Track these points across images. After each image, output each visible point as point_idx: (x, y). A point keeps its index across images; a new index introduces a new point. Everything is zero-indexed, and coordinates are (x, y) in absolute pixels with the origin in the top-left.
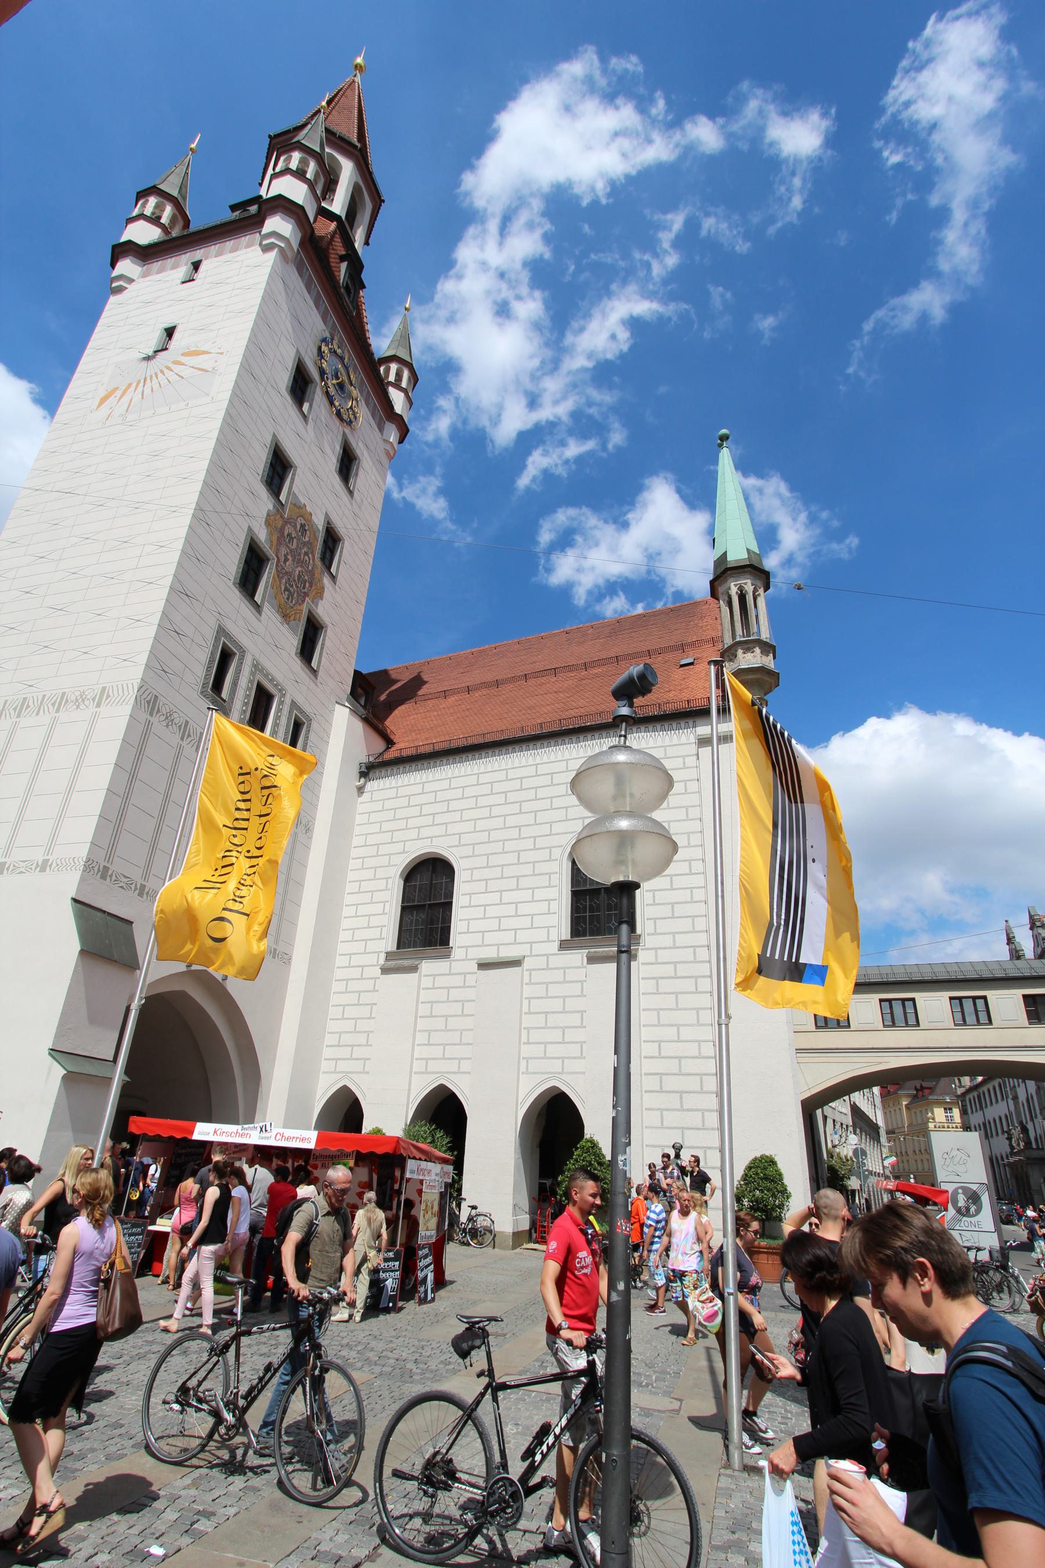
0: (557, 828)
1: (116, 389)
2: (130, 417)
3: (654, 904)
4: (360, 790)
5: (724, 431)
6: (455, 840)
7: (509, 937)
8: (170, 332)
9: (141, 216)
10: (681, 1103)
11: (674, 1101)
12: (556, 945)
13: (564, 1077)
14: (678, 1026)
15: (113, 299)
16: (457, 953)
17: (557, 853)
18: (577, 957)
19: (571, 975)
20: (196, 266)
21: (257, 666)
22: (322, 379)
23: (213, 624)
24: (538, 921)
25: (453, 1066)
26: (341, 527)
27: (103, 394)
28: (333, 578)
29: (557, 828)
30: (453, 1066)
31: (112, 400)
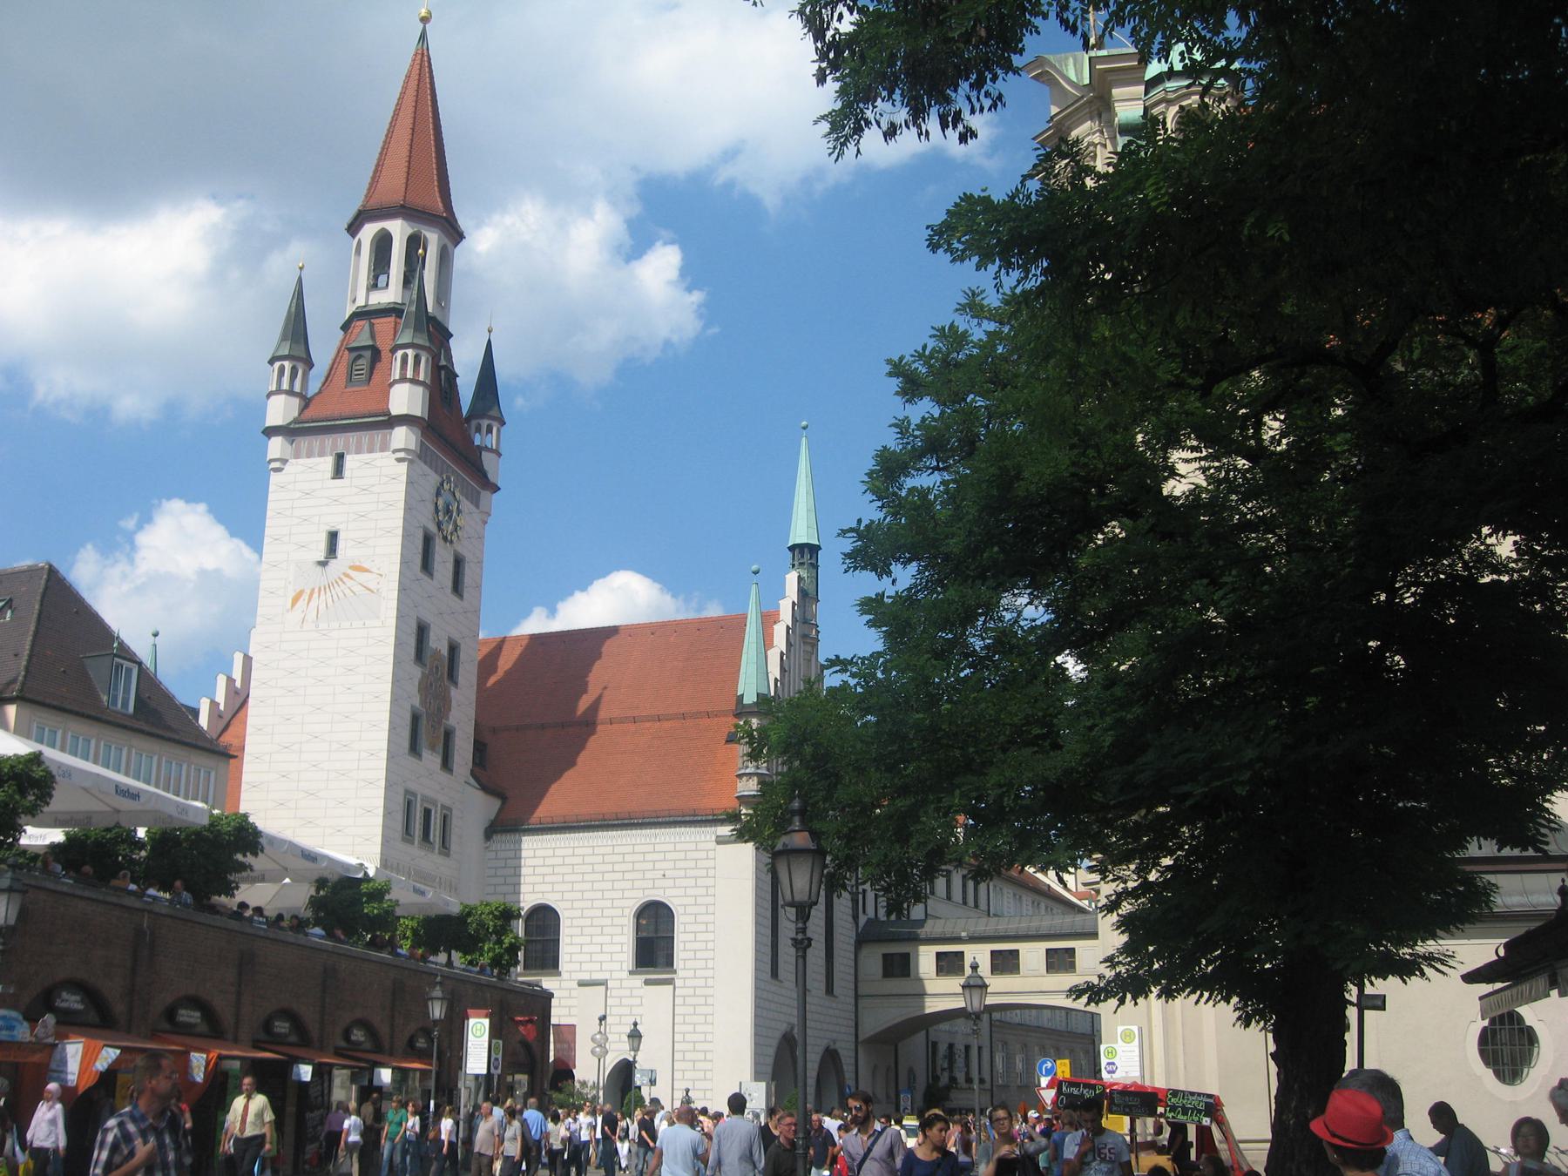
0: (627, 894)
2: (323, 626)
5: (754, 568)
6: (558, 896)
7: (597, 966)
8: (333, 537)
9: (279, 391)
12: (626, 974)
16: (565, 975)
17: (627, 911)
18: (638, 980)
19: (635, 992)
20: (340, 458)
22: (439, 528)
23: (402, 792)
26: (456, 637)
27: (291, 595)
28: (456, 684)
29: (627, 894)
31: (302, 603)
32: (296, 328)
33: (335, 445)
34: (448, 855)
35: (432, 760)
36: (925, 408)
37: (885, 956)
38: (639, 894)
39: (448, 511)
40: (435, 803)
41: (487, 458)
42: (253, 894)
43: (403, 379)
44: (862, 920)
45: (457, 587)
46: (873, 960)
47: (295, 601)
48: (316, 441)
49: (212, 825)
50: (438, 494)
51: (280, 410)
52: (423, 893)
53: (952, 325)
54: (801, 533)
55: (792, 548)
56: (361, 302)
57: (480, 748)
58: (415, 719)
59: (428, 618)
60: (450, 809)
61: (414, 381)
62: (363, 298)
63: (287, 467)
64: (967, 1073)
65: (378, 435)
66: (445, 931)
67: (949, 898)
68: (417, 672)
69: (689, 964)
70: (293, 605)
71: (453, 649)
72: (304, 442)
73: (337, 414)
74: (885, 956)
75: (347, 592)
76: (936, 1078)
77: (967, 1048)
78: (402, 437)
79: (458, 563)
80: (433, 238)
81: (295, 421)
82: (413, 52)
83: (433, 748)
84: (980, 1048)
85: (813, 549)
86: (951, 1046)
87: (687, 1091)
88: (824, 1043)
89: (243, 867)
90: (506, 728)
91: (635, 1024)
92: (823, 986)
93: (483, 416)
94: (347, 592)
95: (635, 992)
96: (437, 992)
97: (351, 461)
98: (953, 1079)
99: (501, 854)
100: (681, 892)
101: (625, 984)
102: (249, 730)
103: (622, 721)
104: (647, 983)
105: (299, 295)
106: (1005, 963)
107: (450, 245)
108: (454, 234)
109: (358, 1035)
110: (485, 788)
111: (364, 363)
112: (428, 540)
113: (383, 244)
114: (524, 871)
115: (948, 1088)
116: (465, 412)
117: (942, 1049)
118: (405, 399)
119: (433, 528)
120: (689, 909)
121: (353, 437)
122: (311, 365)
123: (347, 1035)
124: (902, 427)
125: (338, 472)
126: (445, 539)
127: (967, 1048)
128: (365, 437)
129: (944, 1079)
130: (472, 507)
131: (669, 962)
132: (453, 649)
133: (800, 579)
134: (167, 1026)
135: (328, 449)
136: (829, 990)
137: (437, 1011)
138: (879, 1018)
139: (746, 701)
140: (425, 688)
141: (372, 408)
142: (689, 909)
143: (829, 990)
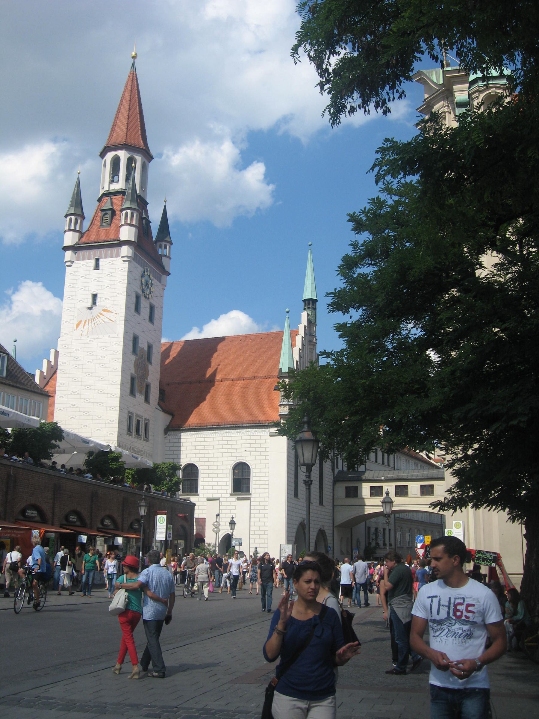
0: (229, 459)
1: (81, 321)
5: (287, 310)
6: (198, 460)
7: (215, 492)
8: (95, 296)
9: (70, 230)
11: (257, 537)
12: (229, 495)
15: (68, 269)
16: (201, 496)
18: (234, 498)
19: (233, 504)
20: (98, 260)
21: (137, 415)
22: (143, 292)
24: (223, 487)
26: (151, 342)
27: (76, 322)
28: (151, 363)
29: (229, 459)
32: (77, 201)
33: (95, 254)
34: (147, 441)
35: (140, 398)
36: (365, 236)
38: (234, 459)
39: (147, 284)
40: (141, 417)
41: (164, 260)
42: (60, 459)
43: (126, 224)
44: (336, 471)
45: (151, 319)
46: (341, 489)
47: (78, 325)
48: (86, 253)
49: (41, 427)
50: (142, 276)
51: (70, 239)
52: (137, 458)
53: (378, 198)
54: (309, 294)
55: (304, 301)
56: (106, 189)
57: (162, 392)
58: (133, 379)
59: (138, 333)
60: (149, 420)
61: (131, 225)
62: (107, 187)
63: (74, 265)
64: (384, 541)
65: (115, 250)
66: (145, 476)
67: (376, 461)
68: (133, 358)
70: (77, 328)
71: (150, 347)
72: (81, 253)
73: (96, 240)
74: (346, 488)
75: (101, 321)
76: (370, 543)
77: (384, 530)
78: (125, 250)
79: (152, 308)
80: (139, 159)
81: (77, 244)
82: (129, 73)
83: (140, 392)
84: (390, 530)
85: (314, 301)
86: (376, 529)
87: (256, 548)
88: (319, 527)
89: (55, 446)
90: (175, 385)
91: (233, 518)
92: (318, 501)
93: (162, 240)
94: (101, 321)
96: (143, 503)
97: (102, 262)
98: (377, 544)
99: (171, 441)
100: (253, 458)
101: (228, 499)
102: (58, 384)
103: (227, 380)
104: (238, 499)
105: (78, 185)
106: (402, 491)
107: (147, 162)
108: (148, 156)
109: (107, 522)
110: (164, 411)
111: (108, 217)
112: (138, 298)
113: (116, 161)
114: (182, 448)
115: (375, 548)
116: (154, 240)
117: (373, 530)
118: (127, 233)
119: (140, 292)
120: (257, 466)
121: (103, 251)
122: (83, 217)
123: (102, 522)
124: (354, 245)
125: (97, 267)
126: (145, 297)
127: (384, 530)
128: (109, 251)
129: (373, 544)
130: (158, 283)
131: (248, 490)
132: (150, 347)
133: (308, 315)
134: (22, 518)
135: (92, 256)
136: (321, 503)
137: (143, 511)
138: (345, 515)
139: (283, 371)
140: (137, 365)
141: (112, 237)
142: (257, 466)
143: (321, 503)
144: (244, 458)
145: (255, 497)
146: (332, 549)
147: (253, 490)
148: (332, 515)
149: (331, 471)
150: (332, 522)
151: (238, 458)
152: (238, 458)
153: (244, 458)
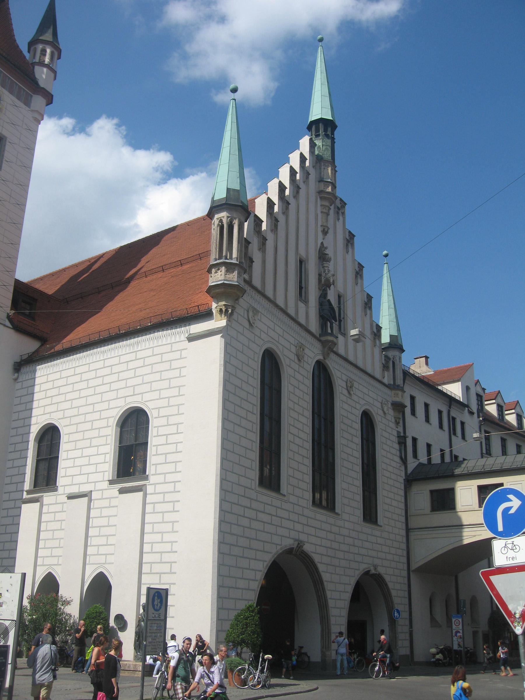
0: (113, 404)
3: (157, 454)
4: (16, 380)
6: (60, 415)
7: (83, 479)
10: (160, 580)
13: (106, 566)
14: (162, 533)
16: (60, 490)
18: (114, 490)
19: (114, 502)
25: (54, 561)
30: (54, 561)
37: (432, 492)
44: (412, 464)
46: (421, 496)
69: (160, 469)
74: (432, 492)
95: (114, 502)
100: (156, 395)
101: (107, 494)
104: (122, 491)
114: (36, 396)
120: (163, 412)
138: (430, 548)
142: (163, 412)
144: (138, 398)
145: (155, 484)
146: (406, 615)
147: (153, 468)
148: (404, 546)
149: (398, 459)
150: (405, 560)
151: (129, 400)
152: (129, 400)
153: (138, 398)
